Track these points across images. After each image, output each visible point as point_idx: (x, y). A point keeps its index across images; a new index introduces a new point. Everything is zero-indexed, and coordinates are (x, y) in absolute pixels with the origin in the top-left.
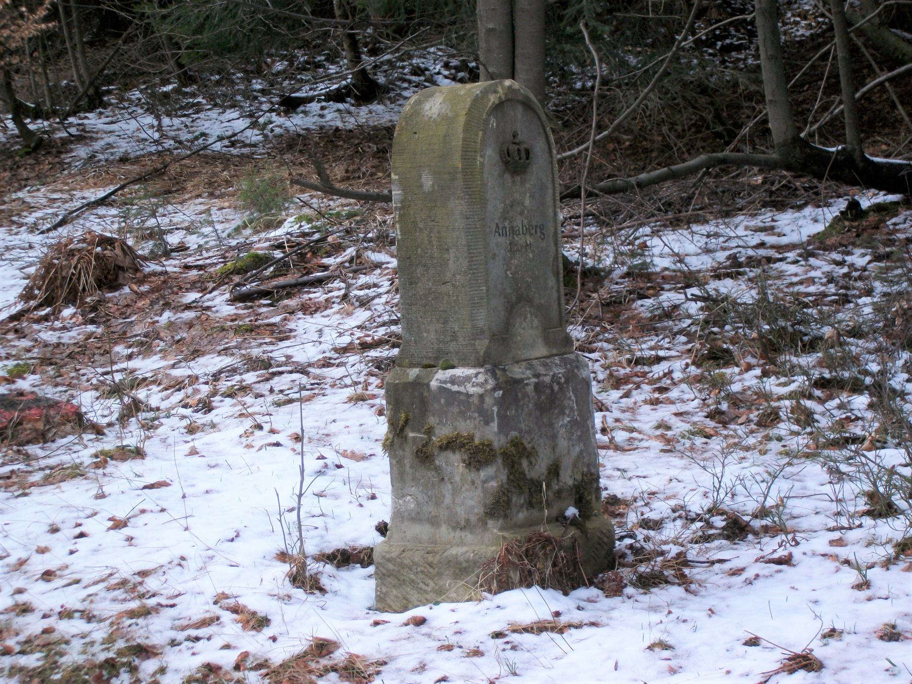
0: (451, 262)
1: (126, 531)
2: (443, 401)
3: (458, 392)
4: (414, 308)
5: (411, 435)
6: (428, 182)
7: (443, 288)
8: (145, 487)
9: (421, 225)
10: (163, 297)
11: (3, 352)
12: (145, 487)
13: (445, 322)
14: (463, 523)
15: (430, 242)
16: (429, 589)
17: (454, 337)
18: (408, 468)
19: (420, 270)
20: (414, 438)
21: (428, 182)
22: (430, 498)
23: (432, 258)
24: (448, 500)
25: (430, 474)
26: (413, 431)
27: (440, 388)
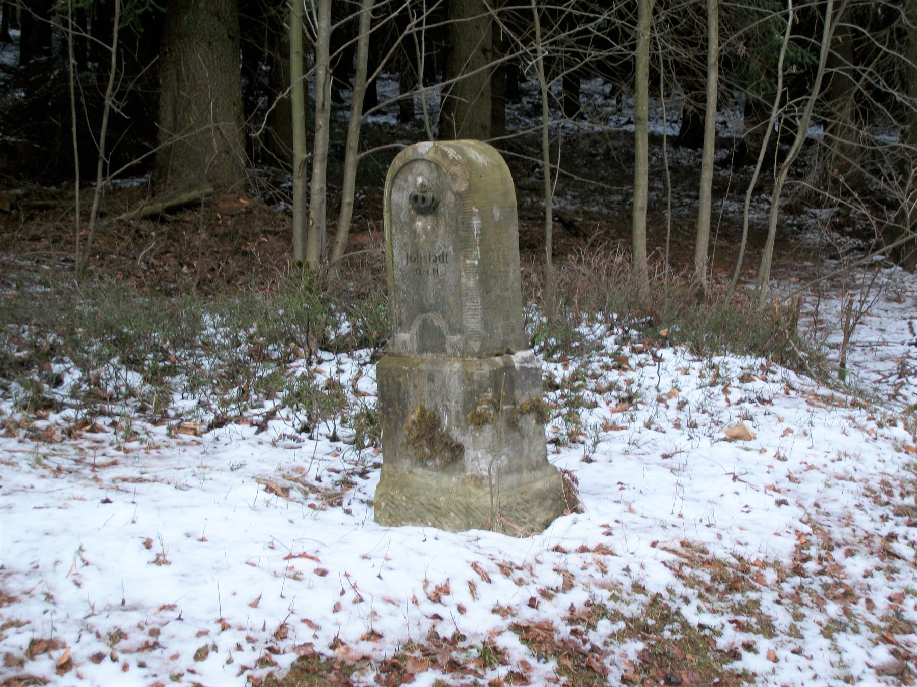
0: (511, 274)
1: (606, 541)
2: (523, 377)
3: (532, 369)
4: (489, 311)
5: (505, 407)
6: (497, 213)
7: (507, 294)
8: (35, 508)
9: (493, 247)
10: (111, 378)
11: (915, 294)
12: (35, 508)
13: (508, 319)
14: (535, 465)
15: (498, 259)
16: (526, 520)
17: (513, 330)
18: (503, 435)
19: (492, 281)
20: (507, 410)
21: (497, 213)
22: (516, 452)
23: (500, 271)
24: (526, 451)
25: (516, 434)
26: (506, 404)
27: (522, 368)
